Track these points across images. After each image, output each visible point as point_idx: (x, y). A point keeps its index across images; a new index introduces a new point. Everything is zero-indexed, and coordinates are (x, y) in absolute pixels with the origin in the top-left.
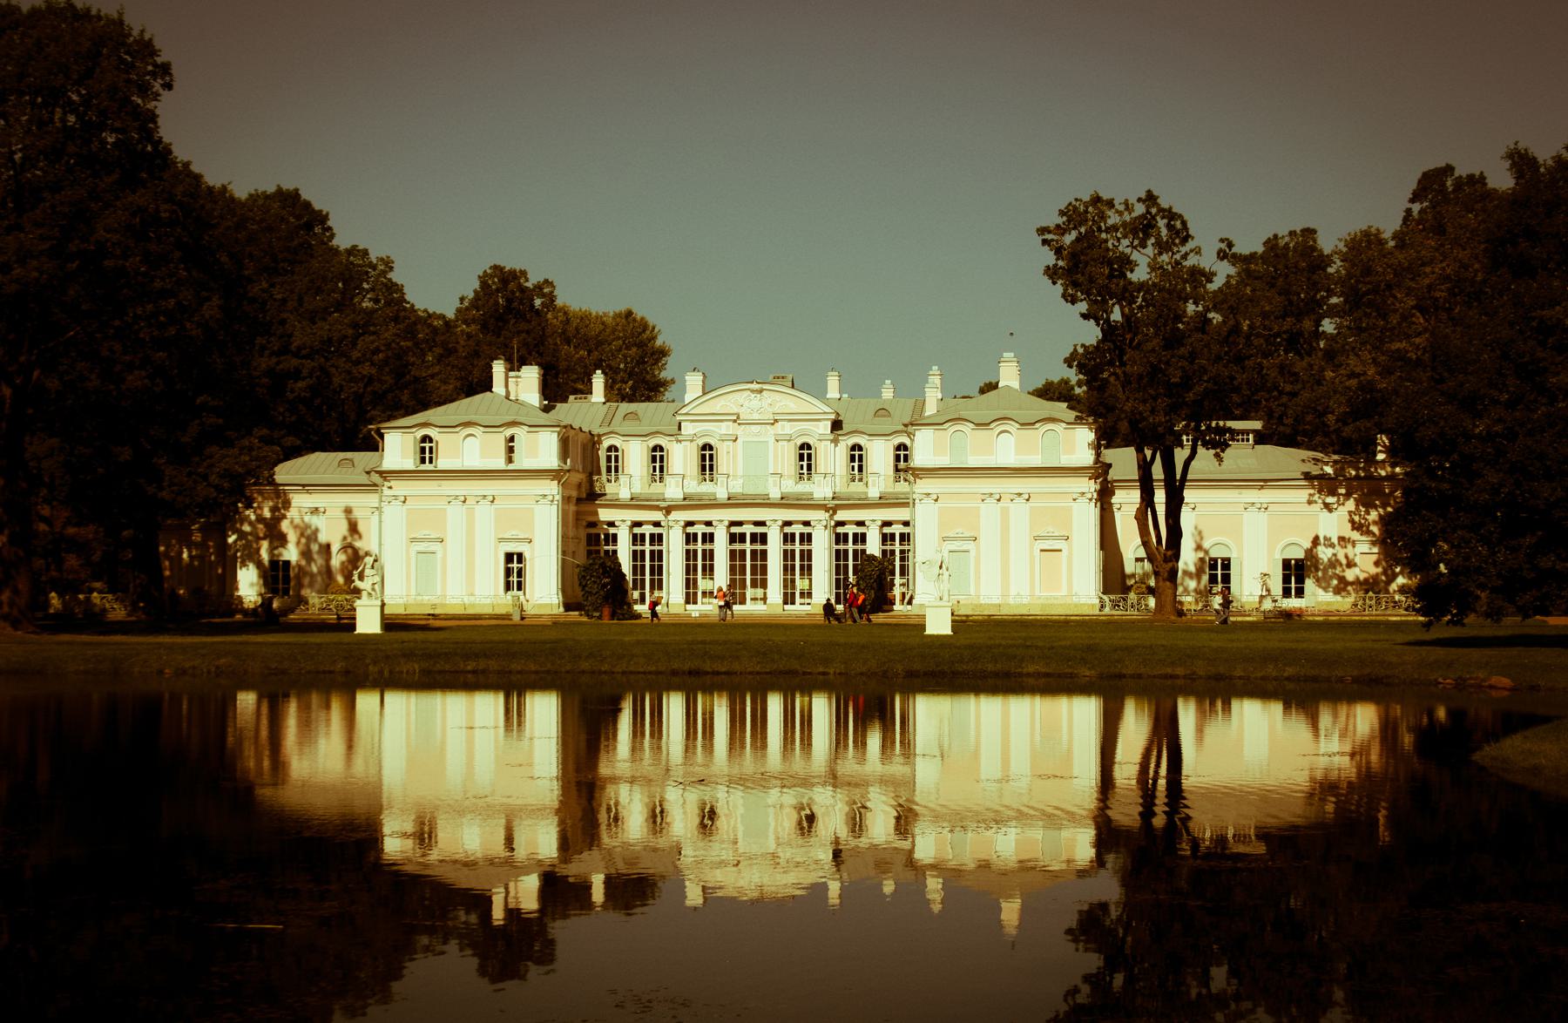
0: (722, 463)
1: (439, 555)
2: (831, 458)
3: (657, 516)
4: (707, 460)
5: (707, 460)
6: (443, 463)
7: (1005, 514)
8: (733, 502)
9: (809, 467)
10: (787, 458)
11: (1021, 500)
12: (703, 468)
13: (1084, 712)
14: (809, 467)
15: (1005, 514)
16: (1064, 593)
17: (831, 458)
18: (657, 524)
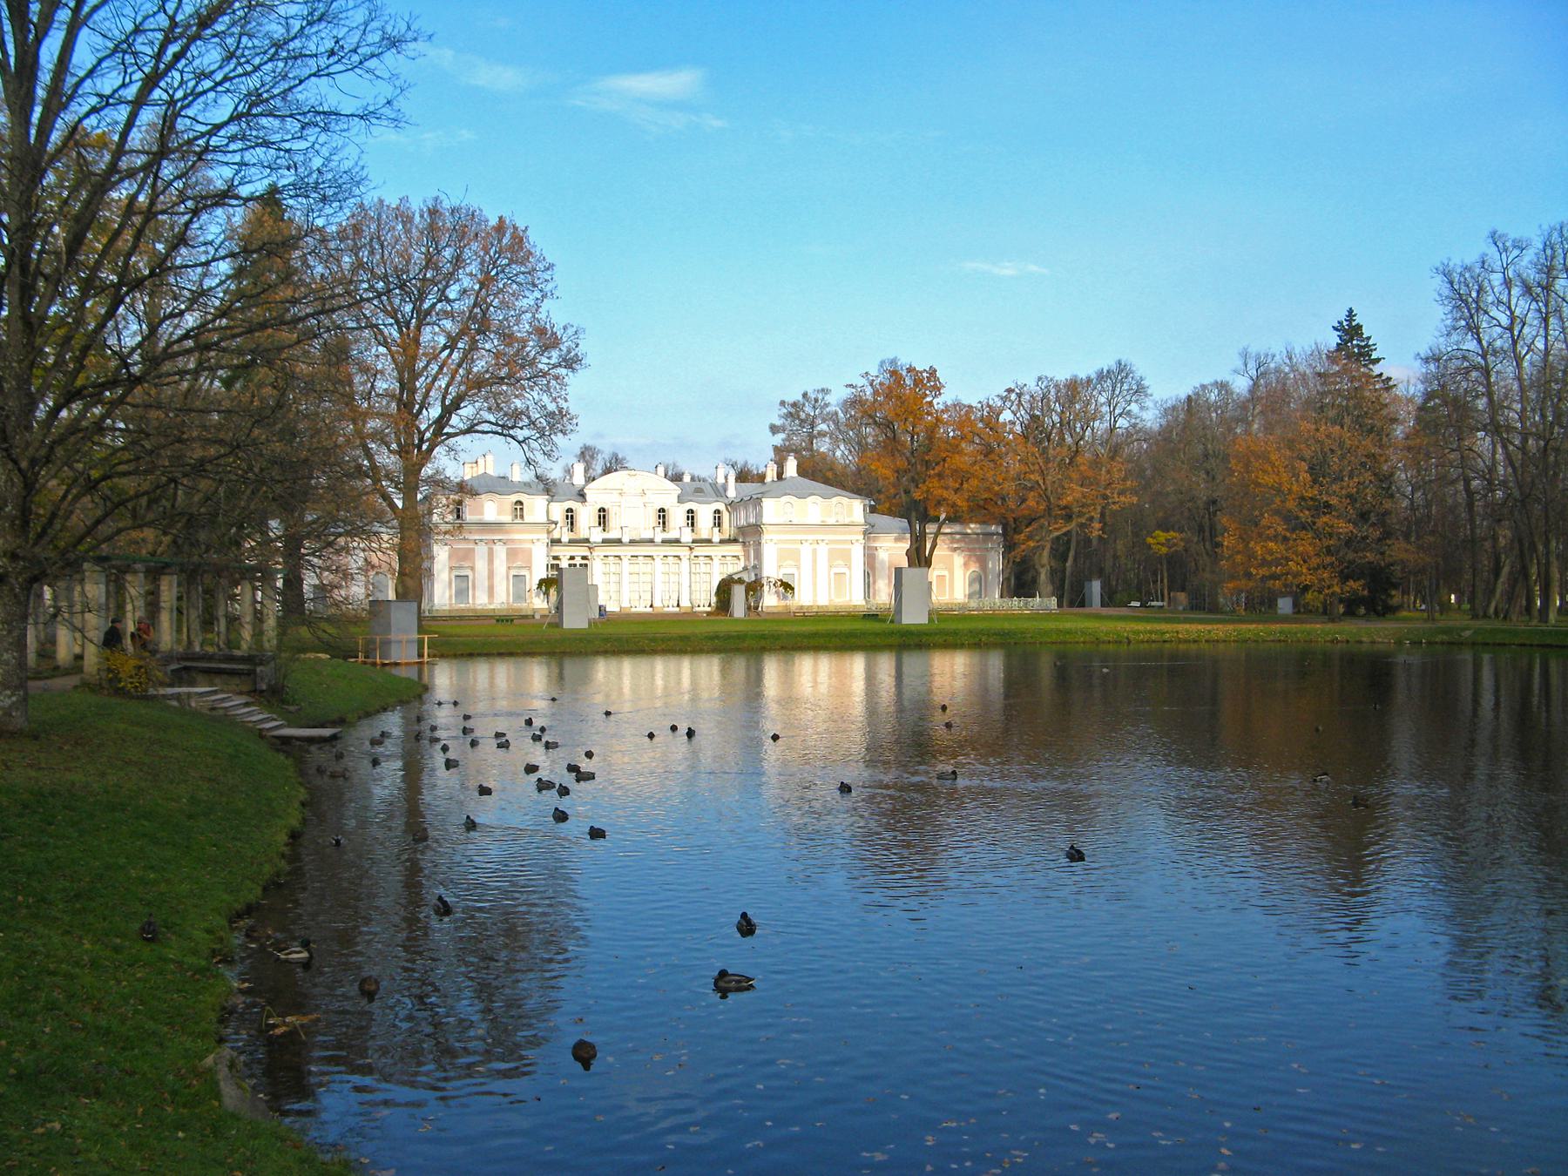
0: (613, 521)
1: (471, 578)
2: (677, 516)
3: (586, 552)
4: (603, 517)
5: (603, 517)
6: (469, 516)
7: (815, 551)
8: (632, 542)
9: (664, 523)
10: (653, 518)
11: (824, 544)
12: (600, 524)
13: (857, 664)
14: (664, 523)
15: (815, 551)
16: (848, 599)
17: (677, 516)
18: (584, 558)
